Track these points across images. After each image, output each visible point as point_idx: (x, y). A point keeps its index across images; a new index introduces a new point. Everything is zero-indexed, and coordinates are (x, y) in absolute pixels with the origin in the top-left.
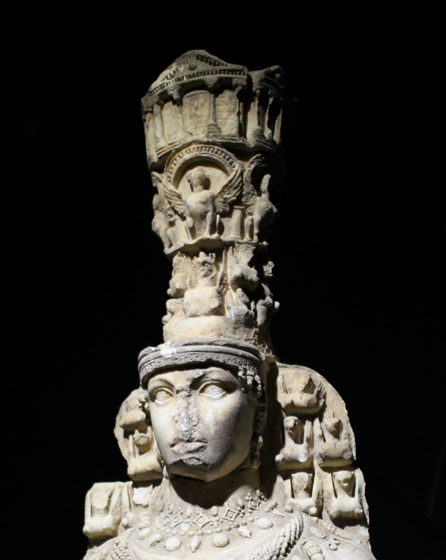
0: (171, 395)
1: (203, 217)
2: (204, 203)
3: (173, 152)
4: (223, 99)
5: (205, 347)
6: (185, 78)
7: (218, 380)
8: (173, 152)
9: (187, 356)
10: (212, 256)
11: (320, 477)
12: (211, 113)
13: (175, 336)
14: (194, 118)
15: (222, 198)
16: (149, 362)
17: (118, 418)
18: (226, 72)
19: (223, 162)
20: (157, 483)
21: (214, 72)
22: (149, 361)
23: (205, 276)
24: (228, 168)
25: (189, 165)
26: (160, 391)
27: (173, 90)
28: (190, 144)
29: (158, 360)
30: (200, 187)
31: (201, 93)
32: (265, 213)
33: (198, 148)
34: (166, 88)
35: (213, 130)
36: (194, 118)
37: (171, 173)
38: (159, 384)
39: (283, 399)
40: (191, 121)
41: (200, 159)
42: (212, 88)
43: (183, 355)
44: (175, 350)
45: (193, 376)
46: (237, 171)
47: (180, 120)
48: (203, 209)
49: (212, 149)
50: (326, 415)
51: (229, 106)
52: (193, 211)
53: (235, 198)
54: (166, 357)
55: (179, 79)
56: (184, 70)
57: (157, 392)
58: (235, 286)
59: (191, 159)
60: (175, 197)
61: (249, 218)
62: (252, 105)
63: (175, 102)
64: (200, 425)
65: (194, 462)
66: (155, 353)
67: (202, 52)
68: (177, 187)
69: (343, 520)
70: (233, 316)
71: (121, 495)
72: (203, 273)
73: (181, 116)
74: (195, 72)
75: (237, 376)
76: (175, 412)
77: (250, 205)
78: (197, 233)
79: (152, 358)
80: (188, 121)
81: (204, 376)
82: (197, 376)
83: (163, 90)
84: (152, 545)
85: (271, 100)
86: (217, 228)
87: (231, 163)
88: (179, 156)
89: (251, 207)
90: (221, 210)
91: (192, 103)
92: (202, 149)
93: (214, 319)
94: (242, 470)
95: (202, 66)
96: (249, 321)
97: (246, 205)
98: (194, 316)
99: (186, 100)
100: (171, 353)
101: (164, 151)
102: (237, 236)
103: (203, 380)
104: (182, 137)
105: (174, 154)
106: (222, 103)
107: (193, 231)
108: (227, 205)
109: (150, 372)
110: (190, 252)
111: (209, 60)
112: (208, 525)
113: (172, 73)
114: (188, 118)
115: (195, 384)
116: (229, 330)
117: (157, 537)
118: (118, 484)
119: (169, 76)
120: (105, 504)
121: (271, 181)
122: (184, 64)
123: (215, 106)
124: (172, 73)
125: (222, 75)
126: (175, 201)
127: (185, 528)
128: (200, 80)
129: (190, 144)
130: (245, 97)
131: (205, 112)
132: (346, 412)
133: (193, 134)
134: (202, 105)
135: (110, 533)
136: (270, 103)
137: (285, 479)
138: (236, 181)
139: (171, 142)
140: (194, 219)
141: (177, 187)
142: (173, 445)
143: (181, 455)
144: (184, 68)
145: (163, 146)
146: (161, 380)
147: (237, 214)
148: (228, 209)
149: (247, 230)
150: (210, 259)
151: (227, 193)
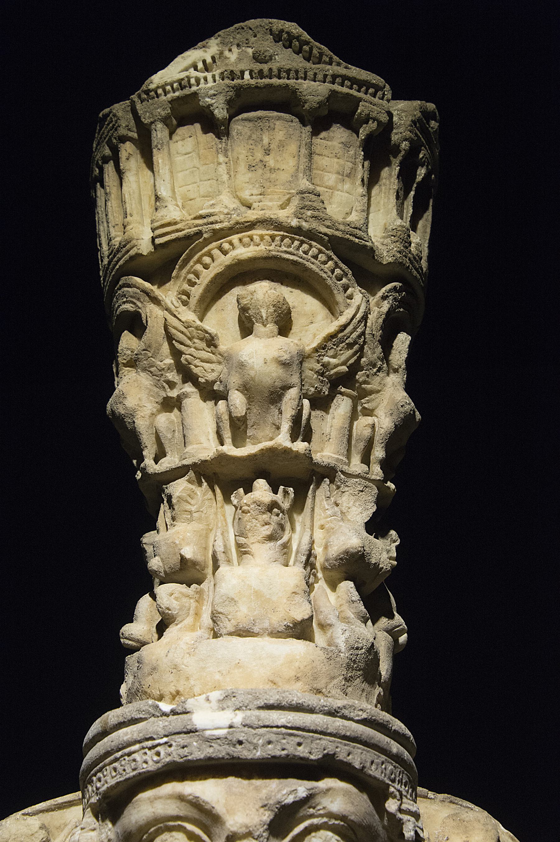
1: (275, 396)
2: (285, 365)
3: (205, 236)
4: (329, 143)
6: (247, 76)
7: (343, 818)
8: (205, 236)
9: (273, 737)
10: (286, 493)
12: (302, 167)
13: (188, 679)
14: (260, 171)
15: (318, 362)
16: (150, 743)
18: (347, 83)
19: (329, 282)
21: (320, 77)
22: (152, 739)
23: (271, 538)
24: (340, 297)
25: (241, 274)
26: (170, 829)
27: (215, 95)
28: (252, 225)
29: (181, 739)
30: (272, 327)
31: (279, 118)
32: (402, 416)
34: (194, 88)
35: (315, 204)
36: (260, 171)
37: (192, 284)
38: (172, 809)
40: (250, 175)
41: (271, 265)
43: (261, 735)
44: (238, 718)
45: (279, 796)
46: (358, 308)
47: (222, 169)
48: (279, 378)
49: (305, 247)
51: (341, 161)
52: (253, 379)
53: (344, 368)
54: (208, 733)
55: (232, 75)
56: (239, 60)
58: (335, 575)
59: (252, 260)
60: (196, 341)
62: (385, 172)
66: (171, 718)
68: (201, 320)
70: (343, 646)
72: (267, 531)
73: (227, 160)
77: (371, 392)
78: (250, 432)
79: (162, 732)
80: (243, 176)
81: (308, 800)
82: (290, 799)
83: (187, 91)
85: (421, 172)
86: (301, 430)
87: (346, 288)
88: (220, 248)
89: (373, 396)
90: (313, 389)
91: (254, 136)
92: (282, 240)
93: (297, 647)
95: (284, 58)
96: (364, 667)
97: (364, 389)
98: (243, 632)
99: (239, 127)
100: (227, 724)
101: (177, 231)
102: (341, 457)
103: (302, 813)
104: (232, 206)
105: (207, 242)
106: (326, 152)
107: (239, 428)
108: (325, 379)
109: (148, 772)
110: (224, 477)
111: (306, 48)
113: (209, 60)
114: (242, 168)
116: (335, 681)
121: (412, 347)
122: (238, 45)
123: (311, 155)
124: (209, 60)
129: (252, 225)
130: (377, 151)
131: (287, 162)
133: (255, 205)
134: (282, 145)
136: (419, 178)
138: (355, 329)
139: (202, 212)
140: (250, 400)
141: (201, 320)
144: (239, 54)
145: (178, 219)
146: (181, 798)
147: (341, 406)
150: (284, 498)
151: (331, 353)
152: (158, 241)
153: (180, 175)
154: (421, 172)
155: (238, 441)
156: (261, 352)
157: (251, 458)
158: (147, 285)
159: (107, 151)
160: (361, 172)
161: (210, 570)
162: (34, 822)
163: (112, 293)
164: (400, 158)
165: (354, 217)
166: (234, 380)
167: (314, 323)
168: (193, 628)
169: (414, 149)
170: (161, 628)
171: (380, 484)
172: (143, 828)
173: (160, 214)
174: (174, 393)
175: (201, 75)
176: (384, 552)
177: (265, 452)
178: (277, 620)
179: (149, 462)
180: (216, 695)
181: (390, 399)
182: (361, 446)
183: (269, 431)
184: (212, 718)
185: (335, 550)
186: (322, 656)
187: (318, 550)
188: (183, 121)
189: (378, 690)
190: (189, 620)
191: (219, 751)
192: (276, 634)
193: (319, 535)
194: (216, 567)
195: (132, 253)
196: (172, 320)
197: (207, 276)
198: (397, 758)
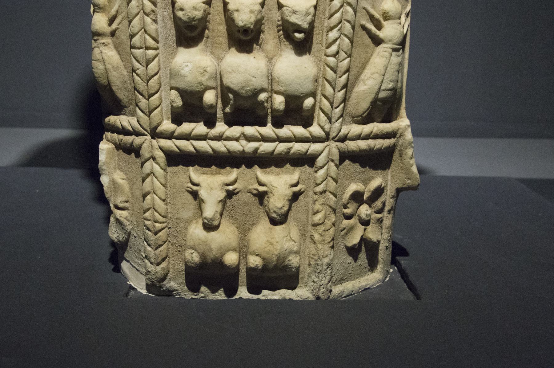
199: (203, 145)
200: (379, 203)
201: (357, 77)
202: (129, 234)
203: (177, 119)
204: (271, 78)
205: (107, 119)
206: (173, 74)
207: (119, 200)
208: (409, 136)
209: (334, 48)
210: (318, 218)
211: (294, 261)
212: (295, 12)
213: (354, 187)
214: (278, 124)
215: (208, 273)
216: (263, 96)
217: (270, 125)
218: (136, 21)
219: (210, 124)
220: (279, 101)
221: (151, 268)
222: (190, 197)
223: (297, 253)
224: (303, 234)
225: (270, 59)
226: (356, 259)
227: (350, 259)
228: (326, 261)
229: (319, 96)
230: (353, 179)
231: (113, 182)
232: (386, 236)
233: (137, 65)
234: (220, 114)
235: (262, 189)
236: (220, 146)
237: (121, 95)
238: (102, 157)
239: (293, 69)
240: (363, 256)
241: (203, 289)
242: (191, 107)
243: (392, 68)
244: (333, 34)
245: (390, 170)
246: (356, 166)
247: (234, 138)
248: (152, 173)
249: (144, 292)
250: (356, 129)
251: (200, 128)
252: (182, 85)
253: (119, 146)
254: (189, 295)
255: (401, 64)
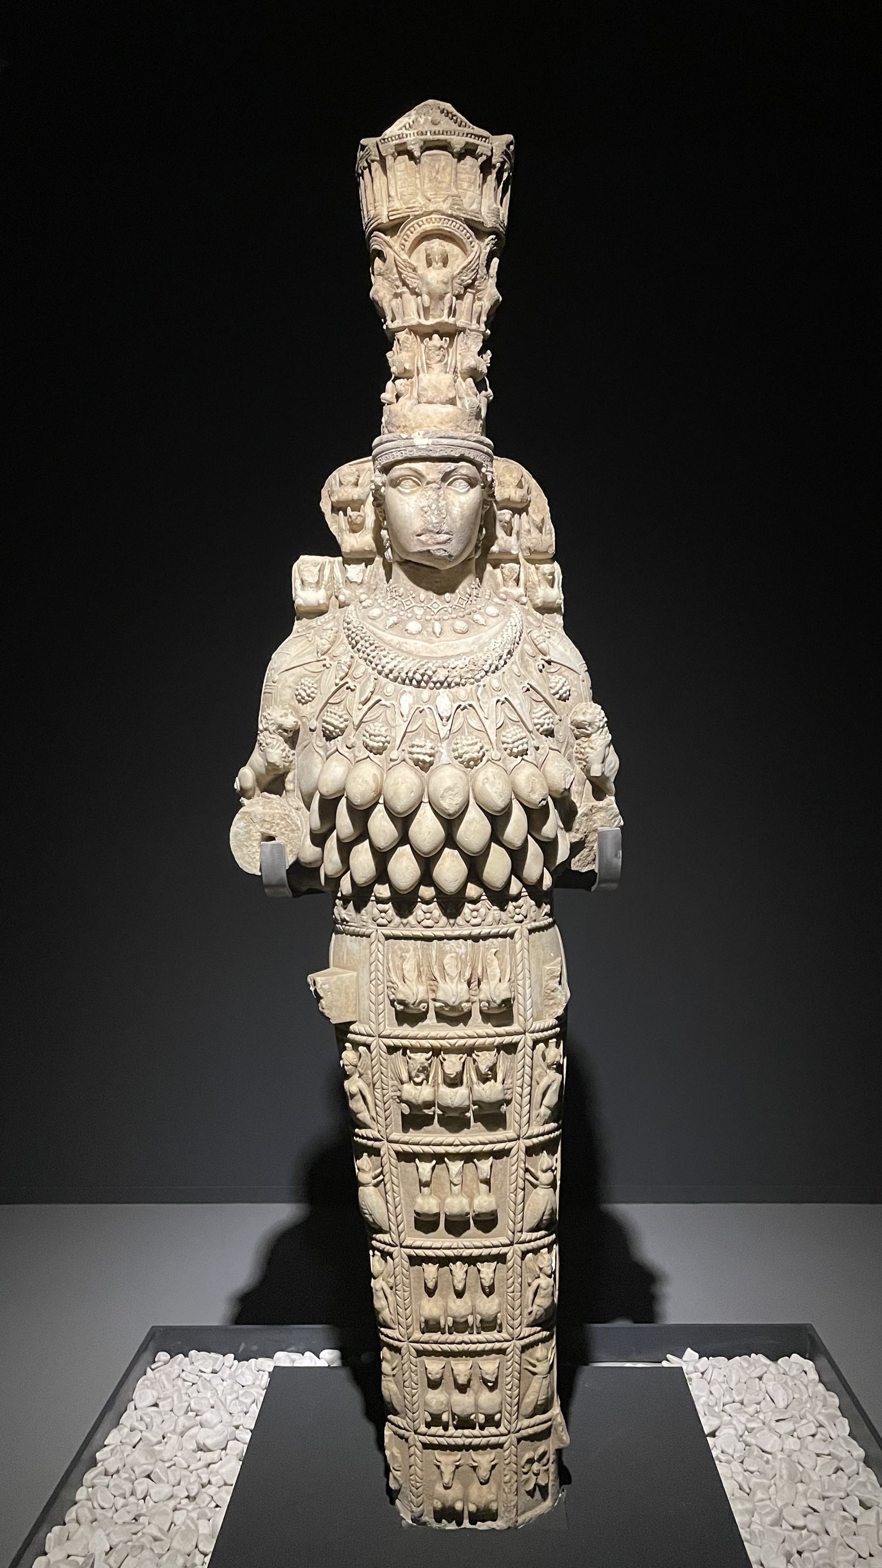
0: (419, 485)
1: (442, 297)
2: (446, 283)
5: (458, 442)
11: (525, 568)
17: (324, 492)
20: (369, 562)
23: (440, 361)
24: (469, 248)
25: (427, 236)
29: (410, 448)
33: (440, 219)
34: (405, 140)
37: (406, 241)
38: (408, 472)
39: (500, 493)
42: (457, 153)
44: (430, 441)
47: (418, 181)
50: (530, 509)
56: (425, 123)
57: (403, 480)
58: (465, 376)
61: (477, 303)
62: (489, 178)
63: (412, 157)
64: (448, 518)
65: (442, 553)
67: (448, 106)
69: (545, 609)
71: (332, 571)
72: (438, 358)
74: (436, 128)
75: (480, 471)
76: (424, 503)
77: (480, 290)
84: (390, 627)
85: (506, 175)
86: (452, 312)
88: (418, 224)
93: (450, 408)
94: (469, 560)
104: (423, 203)
105: (412, 220)
110: (423, 333)
112: (442, 611)
114: (426, 181)
115: (446, 477)
117: (394, 619)
118: (327, 559)
119: (407, 126)
120: (316, 580)
125: (472, 140)
126: (407, 274)
127: (419, 612)
128: (446, 140)
129: (431, 213)
130: (486, 168)
132: (548, 508)
134: (444, 169)
135: (323, 608)
137: (495, 567)
139: (410, 206)
140: (431, 299)
142: (419, 535)
143: (430, 545)
146: (410, 469)
147: (469, 297)
148: (462, 292)
149: (475, 316)
152: (391, 218)
153: (399, 183)
154: (506, 175)
155: (426, 319)
156: (435, 276)
157: (432, 326)
158: (387, 238)
159: (366, 165)
160: (479, 180)
161: (415, 373)
162: (354, 468)
163: (370, 238)
164: (496, 170)
165: (475, 206)
166: (424, 289)
167: (459, 261)
168: (410, 398)
169: (503, 164)
170: (398, 397)
171: (484, 334)
172: (398, 478)
173: (392, 204)
174: (399, 291)
175: (408, 132)
176: (484, 363)
177: (437, 323)
178: (443, 397)
179: (389, 322)
180: (422, 433)
181: (490, 293)
182: (477, 315)
183: (439, 312)
184: (421, 442)
185: (465, 366)
186: (460, 412)
187: (459, 364)
188: (400, 153)
189: (481, 422)
190: (408, 395)
191: (424, 454)
192: (443, 403)
193: (459, 357)
194: (418, 374)
195: (379, 221)
196: (397, 257)
197: (413, 237)
198: (487, 453)
199: (443, 1441)
200: (545, 1460)
201: (524, 1395)
202: (401, 1486)
203: (428, 1425)
204: (476, 1405)
205: (389, 1417)
206: (426, 1404)
207: (396, 1466)
208: (560, 1419)
209: (509, 1386)
210: (507, 1478)
211: (494, 1506)
212: (487, 1374)
213: (527, 1456)
214: (482, 1428)
215: (446, 1513)
216: (472, 1417)
217: (477, 1427)
218: (406, 1374)
219: (446, 1428)
220: (482, 1418)
221: (414, 1509)
222: (436, 1468)
223: (496, 1500)
224: (499, 1487)
225: (476, 1394)
226: (532, 1497)
227: (529, 1498)
228: (513, 1503)
229: (503, 1410)
230: (525, 1450)
231: (392, 1454)
232: (551, 1478)
233: (407, 1396)
234: (450, 1423)
235: (475, 1464)
236: (451, 1441)
237: (398, 1408)
238: (386, 1440)
239: (488, 1400)
240: (538, 1494)
241: (444, 1521)
242: (435, 1420)
243: (544, 1389)
244: (509, 1379)
245: (550, 1439)
246: (529, 1442)
247: (458, 1436)
248: (415, 1454)
249: (410, 1522)
250: (526, 1422)
251: (440, 1430)
252: (431, 1411)
253: (395, 1433)
254: (435, 1525)
255: (550, 1384)
